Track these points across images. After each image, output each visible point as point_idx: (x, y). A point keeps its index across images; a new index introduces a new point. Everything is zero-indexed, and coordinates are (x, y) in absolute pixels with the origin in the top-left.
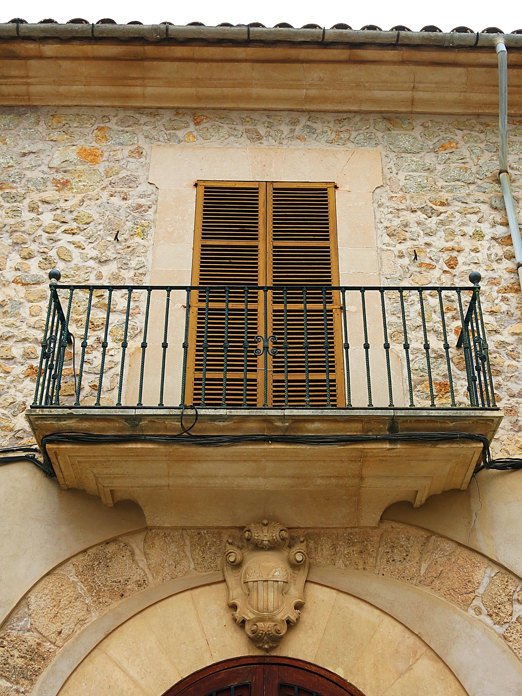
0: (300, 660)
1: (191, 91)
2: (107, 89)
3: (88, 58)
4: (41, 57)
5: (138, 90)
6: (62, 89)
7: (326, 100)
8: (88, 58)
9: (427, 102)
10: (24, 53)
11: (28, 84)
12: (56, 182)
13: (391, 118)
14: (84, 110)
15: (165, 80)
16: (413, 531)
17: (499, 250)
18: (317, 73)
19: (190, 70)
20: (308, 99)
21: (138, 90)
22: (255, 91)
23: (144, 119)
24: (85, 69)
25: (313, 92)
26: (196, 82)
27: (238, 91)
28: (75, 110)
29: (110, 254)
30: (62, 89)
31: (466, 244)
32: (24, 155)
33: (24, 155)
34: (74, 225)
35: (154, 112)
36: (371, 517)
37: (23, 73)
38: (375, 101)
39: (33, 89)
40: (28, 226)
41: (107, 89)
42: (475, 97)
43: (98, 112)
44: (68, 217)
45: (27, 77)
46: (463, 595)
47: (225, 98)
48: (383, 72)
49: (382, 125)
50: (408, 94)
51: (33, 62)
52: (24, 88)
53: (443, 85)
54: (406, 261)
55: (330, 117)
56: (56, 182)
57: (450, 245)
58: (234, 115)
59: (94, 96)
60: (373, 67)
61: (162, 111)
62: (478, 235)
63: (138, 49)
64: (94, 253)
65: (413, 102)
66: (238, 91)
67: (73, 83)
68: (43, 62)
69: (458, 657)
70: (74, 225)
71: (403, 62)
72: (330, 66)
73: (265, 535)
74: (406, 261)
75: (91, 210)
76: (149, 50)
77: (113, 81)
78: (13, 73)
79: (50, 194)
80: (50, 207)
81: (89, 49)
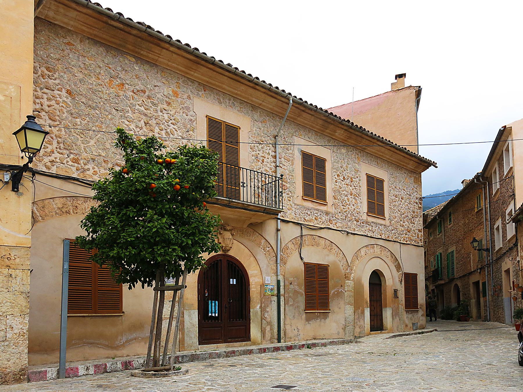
0: (425, 260)
1: (208, 79)
2: (183, 69)
3: (182, 56)
4: (167, 50)
5: (192, 73)
6: (170, 63)
7: (241, 96)
8: (182, 56)
9: (264, 106)
10: (163, 46)
11: (159, 57)
12: (167, 102)
13: (254, 107)
14: (172, 72)
15: (201, 73)
16: (251, 230)
17: (272, 159)
18: (243, 87)
19: (210, 73)
20: (236, 94)
21: (192, 73)
22: (224, 86)
23: (190, 83)
24: (180, 59)
25: (239, 92)
26: (210, 77)
27: (220, 84)
28: (169, 71)
29: (185, 136)
30: (170, 63)
31: (267, 156)
32: (155, 86)
33: (155, 86)
34: (174, 122)
35: (193, 81)
36: (245, 226)
37: (159, 53)
38: (252, 101)
39: (160, 59)
40: (160, 118)
41: (183, 69)
42: (275, 108)
43: (176, 75)
44: (172, 118)
45: (160, 54)
46: (259, 245)
47: (214, 85)
48: (259, 94)
49: (251, 109)
50: (261, 102)
51: (164, 50)
52: (157, 58)
53: (271, 103)
54: (254, 158)
55: (239, 101)
56: (167, 102)
57: (263, 155)
58: (215, 91)
59: (178, 69)
60: (257, 91)
61: (195, 82)
62: (269, 154)
63: (200, 60)
64: (180, 134)
65: (260, 104)
66: (220, 84)
67: (174, 63)
68: (168, 52)
69: (258, 257)
70: (174, 122)
71: (264, 93)
72: (247, 87)
73: (228, 228)
74: (254, 158)
75: (178, 117)
76: (203, 62)
77: (186, 67)
78: (156, 51)
79: (165, 106)
80: (167, 112)
81: (185, 54)
